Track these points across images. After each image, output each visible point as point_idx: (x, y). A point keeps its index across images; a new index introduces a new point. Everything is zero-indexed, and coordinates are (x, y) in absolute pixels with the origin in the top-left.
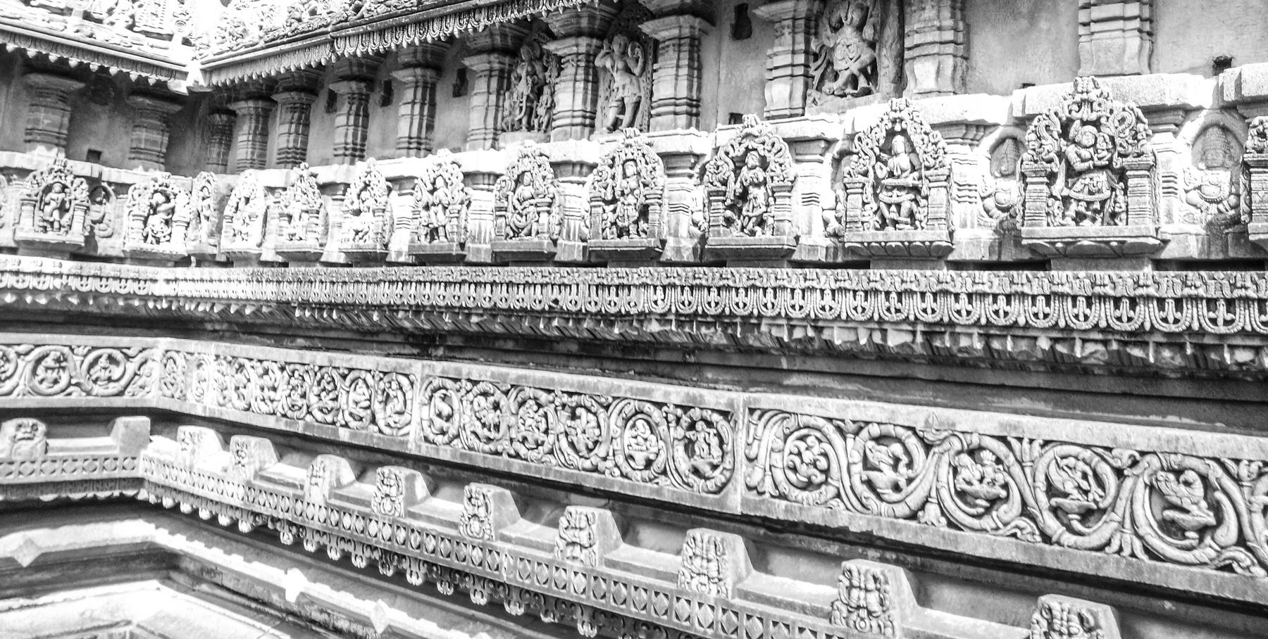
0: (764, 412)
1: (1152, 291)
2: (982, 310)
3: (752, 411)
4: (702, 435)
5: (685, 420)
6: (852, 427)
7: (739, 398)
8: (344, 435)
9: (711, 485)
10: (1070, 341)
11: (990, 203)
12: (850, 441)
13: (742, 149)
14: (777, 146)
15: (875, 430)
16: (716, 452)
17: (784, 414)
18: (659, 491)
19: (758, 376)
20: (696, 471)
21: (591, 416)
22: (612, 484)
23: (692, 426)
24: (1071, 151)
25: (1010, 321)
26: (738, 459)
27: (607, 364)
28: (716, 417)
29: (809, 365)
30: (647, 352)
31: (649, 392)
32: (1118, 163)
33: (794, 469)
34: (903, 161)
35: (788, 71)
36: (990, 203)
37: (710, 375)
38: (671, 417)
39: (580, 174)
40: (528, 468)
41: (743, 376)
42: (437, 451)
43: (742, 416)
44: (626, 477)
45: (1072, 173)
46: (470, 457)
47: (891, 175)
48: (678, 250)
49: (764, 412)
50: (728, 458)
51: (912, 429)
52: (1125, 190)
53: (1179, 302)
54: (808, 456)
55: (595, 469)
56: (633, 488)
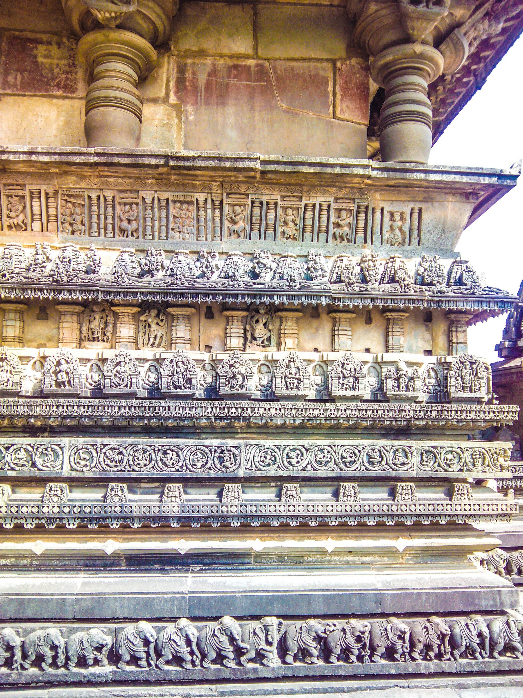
0: (251, 445)
1: (371, 408)
2: (326, 413)
3: (247, 446)
4: (227, 455)
5: (219, 451)
6: (283, 447)
7: (242, 442)
8: (11, 473)
9: (231, 469)
10: (348, 421)
11: (313, 383)
12: (281, 452)
13: (233, 361)
14: (248, 362)
15: (291, 447)
16: (232, 459)
17: (259, 446)
18: (209, 474)
19: (225, 435)
20: (225, 466)
21: (174, 453)
22: (187, 475)
23: (222, 452)
24: (344, 371)
25: (335, 416)
26: (242, 461)
27: (151, 435)
28: (232, 449)
29: (249, 431)
30: (178, 430)
31: (203, 443)
32: (357, 375)
33: (263, 461)
34: (294, 370)
35: (232, 335)
36: (313, 383)
37: (204, 436)
38: (213, 450)
39: (143, 363)
40: (142, 474)
41: (219, 435)
42: (84, 474)
43: (243, 448)
44: (193, 472)
45: (344, 377)
46: (106, 474)
47: (290, 374)
48: (200, 394)
49: (251, 445)
50: (238, 461)
51: (303, 446)
52: (358, 383)
53: (377, 411)
54: (268, 457)
55: (178, 471)
56: (197, 475)
